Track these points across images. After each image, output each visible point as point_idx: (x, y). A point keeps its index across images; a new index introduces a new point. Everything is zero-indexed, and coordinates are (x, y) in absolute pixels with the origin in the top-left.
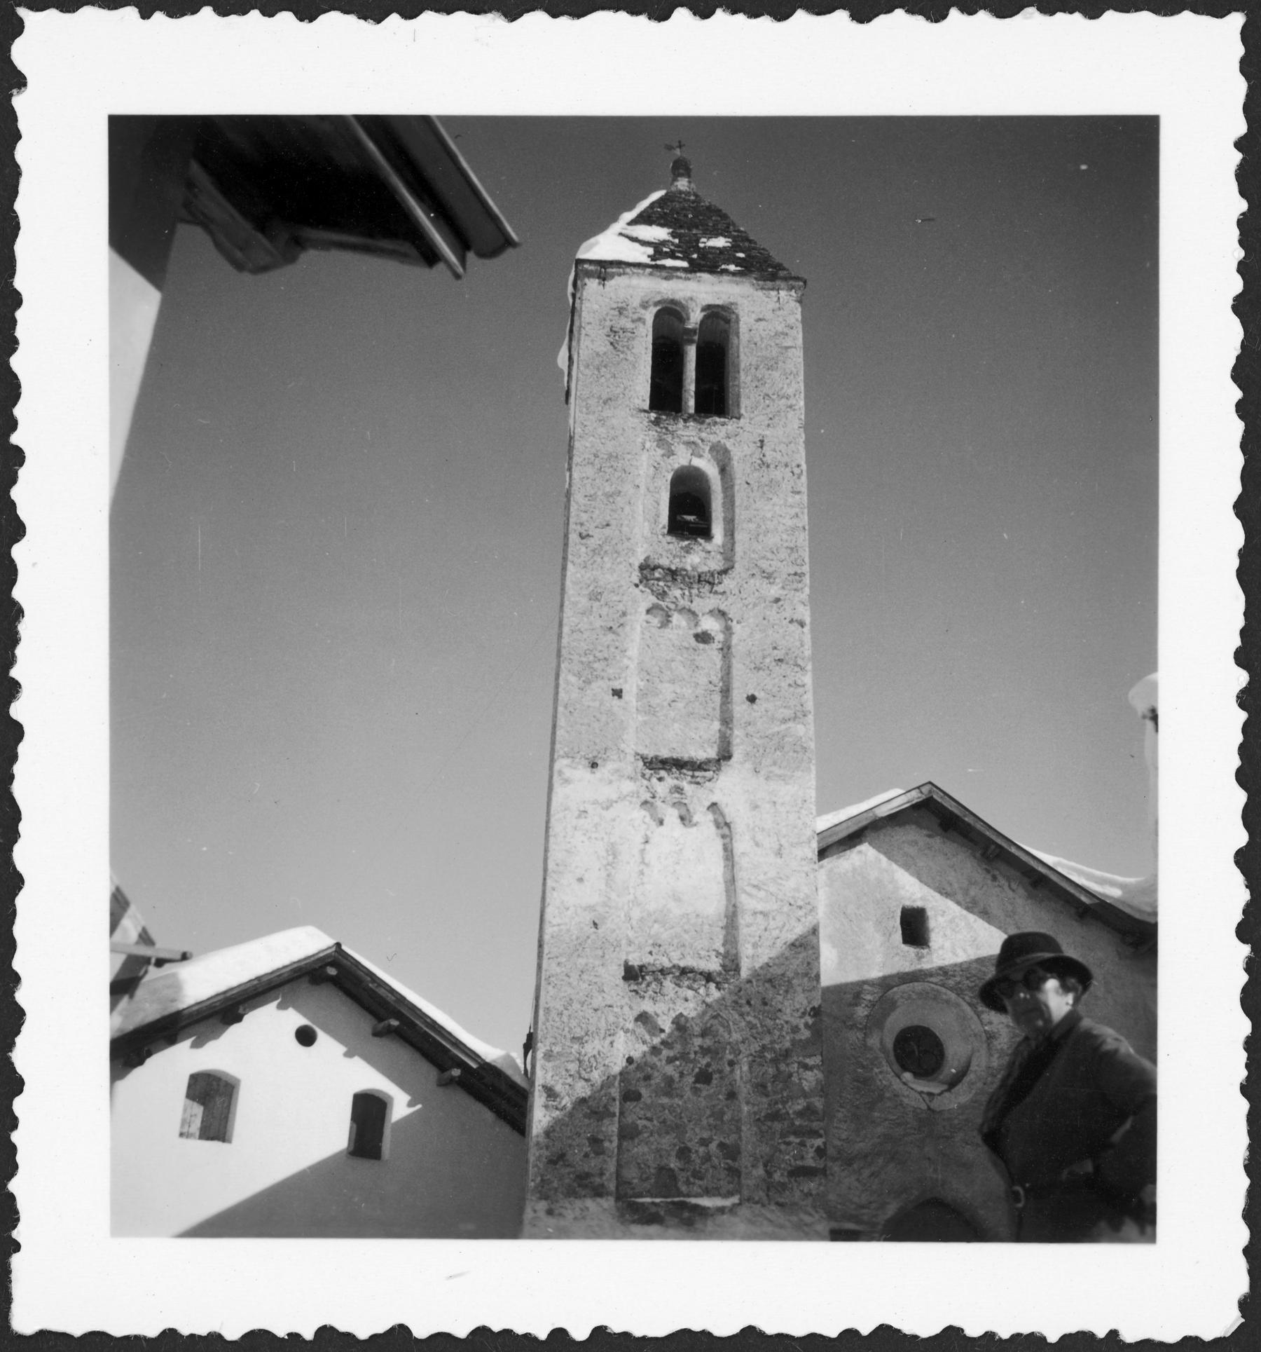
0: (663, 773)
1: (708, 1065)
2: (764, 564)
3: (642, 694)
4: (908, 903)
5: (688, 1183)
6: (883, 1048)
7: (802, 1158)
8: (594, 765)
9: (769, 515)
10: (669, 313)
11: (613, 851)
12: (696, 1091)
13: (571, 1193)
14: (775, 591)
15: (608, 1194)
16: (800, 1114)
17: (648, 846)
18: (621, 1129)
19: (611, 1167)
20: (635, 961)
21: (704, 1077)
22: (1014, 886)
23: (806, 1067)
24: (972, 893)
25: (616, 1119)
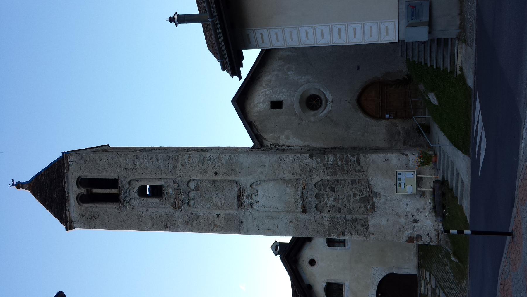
2: (170, 169)
3: (218, 208)
4: (269, 107)
5: (363, 194)
6: (314, 115)
8: (242, 223)
9: (153, 167)
10: (82, 199)
11: (268, 217)
12: (337, 192)
13: (367, 228)
14: (179, 165)
15: (367, 218)
16: (342, 162)
18: (348, 214)
19: (360, 217)
20: (300, 210)
21: (333, 189)
23: (328, 159)
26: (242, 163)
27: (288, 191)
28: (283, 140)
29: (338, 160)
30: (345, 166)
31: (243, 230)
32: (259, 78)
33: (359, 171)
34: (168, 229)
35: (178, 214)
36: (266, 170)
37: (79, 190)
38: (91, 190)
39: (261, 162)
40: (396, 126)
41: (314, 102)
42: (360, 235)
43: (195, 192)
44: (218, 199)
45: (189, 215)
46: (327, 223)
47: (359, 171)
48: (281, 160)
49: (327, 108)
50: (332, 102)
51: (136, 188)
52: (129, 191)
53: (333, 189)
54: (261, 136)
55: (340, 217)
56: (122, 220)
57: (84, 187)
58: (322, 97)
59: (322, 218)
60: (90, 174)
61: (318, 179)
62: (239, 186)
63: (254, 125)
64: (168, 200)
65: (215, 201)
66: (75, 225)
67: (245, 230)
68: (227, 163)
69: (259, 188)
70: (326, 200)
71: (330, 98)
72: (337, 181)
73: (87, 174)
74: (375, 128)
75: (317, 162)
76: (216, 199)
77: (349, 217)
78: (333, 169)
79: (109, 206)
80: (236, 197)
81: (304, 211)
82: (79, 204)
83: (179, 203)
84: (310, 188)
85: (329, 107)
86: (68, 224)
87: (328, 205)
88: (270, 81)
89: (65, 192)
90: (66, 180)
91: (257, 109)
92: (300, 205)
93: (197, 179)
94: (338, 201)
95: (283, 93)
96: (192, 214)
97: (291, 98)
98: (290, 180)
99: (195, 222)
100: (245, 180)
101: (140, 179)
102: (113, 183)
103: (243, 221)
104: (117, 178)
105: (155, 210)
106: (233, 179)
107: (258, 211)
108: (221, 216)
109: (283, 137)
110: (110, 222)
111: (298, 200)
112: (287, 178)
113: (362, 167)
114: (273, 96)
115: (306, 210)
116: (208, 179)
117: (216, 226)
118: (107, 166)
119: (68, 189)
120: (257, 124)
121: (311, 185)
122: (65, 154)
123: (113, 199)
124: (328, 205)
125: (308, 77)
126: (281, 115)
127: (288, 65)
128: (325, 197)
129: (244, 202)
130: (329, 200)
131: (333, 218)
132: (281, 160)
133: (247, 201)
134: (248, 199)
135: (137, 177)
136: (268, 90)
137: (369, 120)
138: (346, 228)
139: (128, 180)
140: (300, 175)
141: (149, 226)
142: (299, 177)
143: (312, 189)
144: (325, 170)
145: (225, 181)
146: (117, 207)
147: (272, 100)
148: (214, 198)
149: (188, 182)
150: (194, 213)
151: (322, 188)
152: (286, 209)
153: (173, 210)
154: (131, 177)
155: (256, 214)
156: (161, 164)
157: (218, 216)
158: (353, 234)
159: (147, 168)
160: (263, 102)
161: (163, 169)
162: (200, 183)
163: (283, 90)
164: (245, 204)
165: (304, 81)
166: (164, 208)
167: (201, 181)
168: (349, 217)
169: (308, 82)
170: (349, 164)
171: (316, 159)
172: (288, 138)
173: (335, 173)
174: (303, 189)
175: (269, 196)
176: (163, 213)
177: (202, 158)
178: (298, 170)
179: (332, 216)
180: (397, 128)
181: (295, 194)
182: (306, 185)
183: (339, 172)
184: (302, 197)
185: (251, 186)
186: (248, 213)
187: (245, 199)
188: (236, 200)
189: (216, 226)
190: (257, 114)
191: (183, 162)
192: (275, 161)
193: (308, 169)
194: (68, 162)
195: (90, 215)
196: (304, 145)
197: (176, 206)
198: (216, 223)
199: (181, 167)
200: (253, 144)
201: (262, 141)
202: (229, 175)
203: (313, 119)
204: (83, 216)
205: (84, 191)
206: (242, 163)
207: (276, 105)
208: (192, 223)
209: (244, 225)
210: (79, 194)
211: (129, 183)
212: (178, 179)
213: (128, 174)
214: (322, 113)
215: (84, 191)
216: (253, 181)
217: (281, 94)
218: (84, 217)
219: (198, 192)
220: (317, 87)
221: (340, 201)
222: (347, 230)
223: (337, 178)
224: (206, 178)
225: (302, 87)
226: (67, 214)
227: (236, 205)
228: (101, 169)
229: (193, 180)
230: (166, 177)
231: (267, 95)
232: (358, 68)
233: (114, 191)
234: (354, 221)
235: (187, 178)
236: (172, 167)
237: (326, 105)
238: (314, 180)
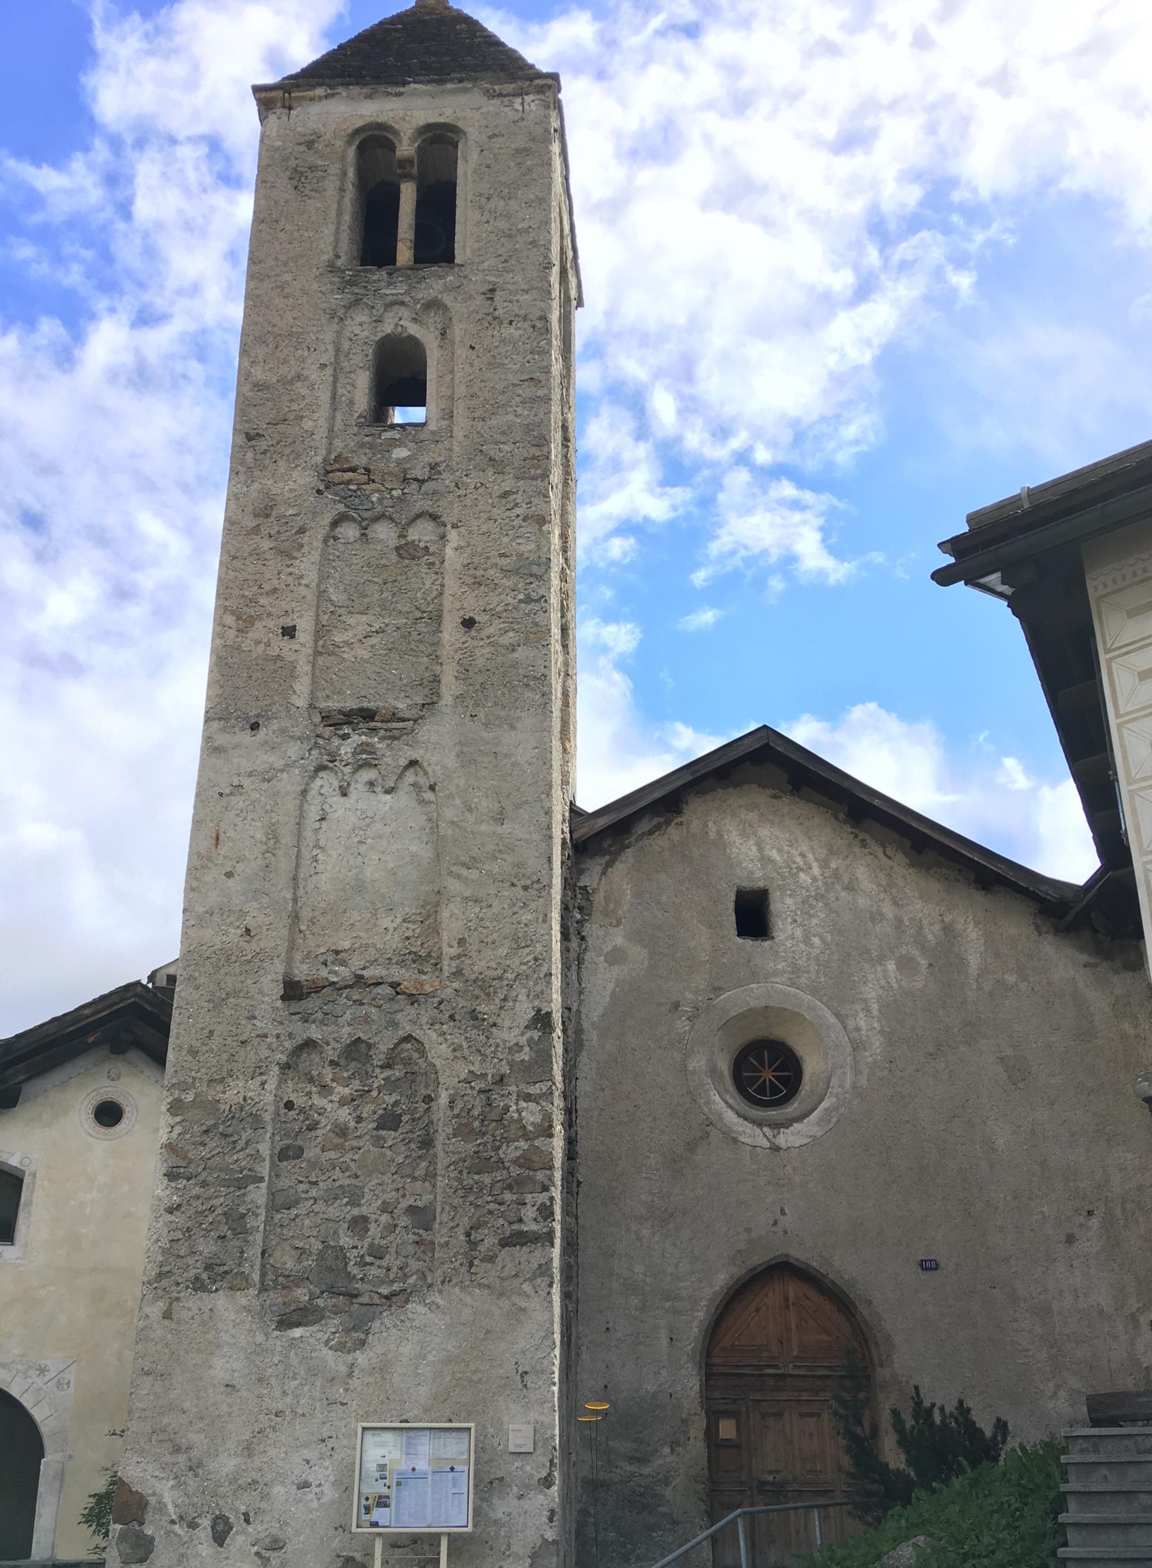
0: (347, 730)
1: (396, 1103)
3: (321, 631)
4: (747, 884)
5: (362, 1264)
6: (713, 1071)
7: (521, 1220)
8: (255, 727)
9: (500, 386)
10: (373, 142)
11: (273, 835)
12: (378, 1142)
13: (198, 1285)
14: (508, 485)
16: (515, 1162)
17: (324, 824)
18: (272, 1194)
19: (254, 1252)
20: (302, 972)
21: (389, 1121)
22: (889, 852)
23: (528, 1098)
24: (833, 865)
25: (264, 1185)
26: (512, 727)
27: (386, 922)
28: (606, 937)
29: (523, 1144)
30: (498, 1175)
31: (223, 730)
32: (864, 844)
33: (473, 1244)
34: (242, 440)
35: (303, 479)
36: (483, 827)
37: (409, 133)
38: (408, 177)
39: (518, 806)
40: (674, 1445)
41: (768, 1075)
42: (164, 1251)
43: (393, 542)
44: (361, 630)
45: (299, 522)
46: (231, 1095)
47: (473, 1244)
48: (525, 888)
49: (748, 1127)
50: (776, 1149)
51: (413, 330)
52: (403, 303)
53: (389, 1121)
54: (624, 847)
55: (257, 1157)
56: (288, 277)
57: (420, 150)
58: (792, 1108)
59: (259, 1070)
60: (472, 165)
61: (438, 1049)
62: (413, 713)
63: (668, 823)
64: (362, 445)
65: (352, 620)
66: (272, 118)
67: (222, 739)
68: (515, 665)
69: (404, 798)
70: (341, 1091)
71: (790, 1138)
72: (427, 1143)
73: (474, 156)
74: (665, 1342)
75: (518, 1047)
76: (359, 623)
77: (258, 1195)
78: (485, 1120)
79: (345, 236)
80: (365, 705)
81: (293, 991)
82: (357, 132)
83: (349, 482)
84: (399, 1016)
85: (752, 1135)
86: (279, 94)
87: (318, 1101)
88: (850, 888)
89: (404, 84)
90: (449, 86)
91: (733, 836)
92: (324, 973)
93: (449, 551)
94: (336, 1147)
95: (807, 941)
96: (302, 531)
97: (784, 974)
98: (435, 930)
99: (266, 544)
100: (437, 742)
101: (452, 342)
102: (436, 245)
103: (262, 732)
104: (457, 261)
105: (325, 397)
106: (444, 689)
107: (304, 793)
108: (286, 644)
109: (618, 938)
110: (282, 235)
111: (343, 963)
112: (445, 914)
113: (491, 1259)
114: (789, 901)
115: (300, 998)
116: (447, 592)
117: (246, 622)
118: (503, 224)
119: (414, 94)
120: (674, 833)
121: (408, 1019)
122: (550, 82)
123: (374, 245)
124: (318, 1101)
125: (876, 1046)
126: (712, 933)
127: (924, 962)
128: (356, 1084)
129: (345, 737)
130: (343, 1102)
131: (256, 1122)
132: (525, 888)
133: (346, 750)
134: (354, 754)
135: (458, 330)
136: (815, 879)
137: (701, 1315)
138: (204, 1184)
139: (447, 299)
140: (458, 973)
141: (259, 374)
142: (448, 967)
143: (395, 1025)
144: (478, 1085)
145: (436, 659)
146: (339, 263)
147: (775, 895)
148: (364, 618)
149: (434, 517)
150: (305, 539)
151: (397, 1073)
152: (305, 914)
153: (319, 459)
154: (457, 307)
155: (289, 783)
156: (511, 417)
157: (289, 632)
158: (178, 1218)
159: (494, 365)
160: (765, 860)
161: (493, 422)
162: (431, 565)
163: (816, 941)
164: (336, 741)
165: (858, 1029)
166: (331, 430)
167: (436, 566)
168: (258, 1195)
169: (857, 1046)
170: (508, 1196)
171: (530, 1041)
172: (616, 957)
173: (463, 1131)
174: (394, 985)
175: (366, 840)
176: (308, 424)
177: (535, 569)
178: (481, 964)
179: (267, 1117)
180: (667, 1450)
181: (372, 953)
182: (413, 999)
183: (471, 1147)
184: (359, 981)
185: (413, 763)
186: (294, 750)
187: (356, 739)
188: (352, 704)
189: (246, 622)
190: (712, 835)
191: (519, 498)
192: (520, 865)
193: (482, 1008)
194: (520, 93)
195: (313, 168)
196: (586, 1025)
197: (334, 475)
198: (258, 625)
199: (497, 490)
200: (590, 809)
201: (602, 852)
202: (465, 672)
203: (698, 1063)
204: (310, 144)
205: (406, 148)
206: (512, 727)
207: (753, 915)
208: (264, 531)
209: (246, 737)
210: (396, 133)
211: (433, 305)
212: (448, 479)
213: (471, 298)
214: (723, 1106)
215: (406, 148)
216: (435, 771)
217: (799, 933)
218: (303, 148)
219: (394, 558)
220: (834, 1082)
221: (332, 1155)
222: (197, 1190)
223: (440, 1139)
224: (452, 585)
225: (832, 1019)
226: (320, 91)
227: (334, 704)
228: (491, 205)
229: (443, 537)
230: (459, 433)
231: (796, 875)
232: (929, 1266)
233: (404, 254)
234: (237, 1222)
235: (451, 511)
236: (498, 456)
237: (759, 1124)
238: (434, 1036)
